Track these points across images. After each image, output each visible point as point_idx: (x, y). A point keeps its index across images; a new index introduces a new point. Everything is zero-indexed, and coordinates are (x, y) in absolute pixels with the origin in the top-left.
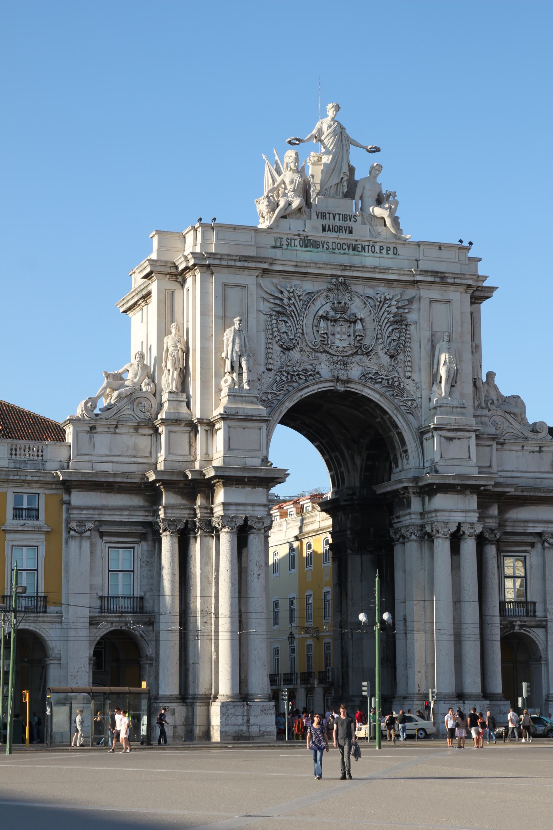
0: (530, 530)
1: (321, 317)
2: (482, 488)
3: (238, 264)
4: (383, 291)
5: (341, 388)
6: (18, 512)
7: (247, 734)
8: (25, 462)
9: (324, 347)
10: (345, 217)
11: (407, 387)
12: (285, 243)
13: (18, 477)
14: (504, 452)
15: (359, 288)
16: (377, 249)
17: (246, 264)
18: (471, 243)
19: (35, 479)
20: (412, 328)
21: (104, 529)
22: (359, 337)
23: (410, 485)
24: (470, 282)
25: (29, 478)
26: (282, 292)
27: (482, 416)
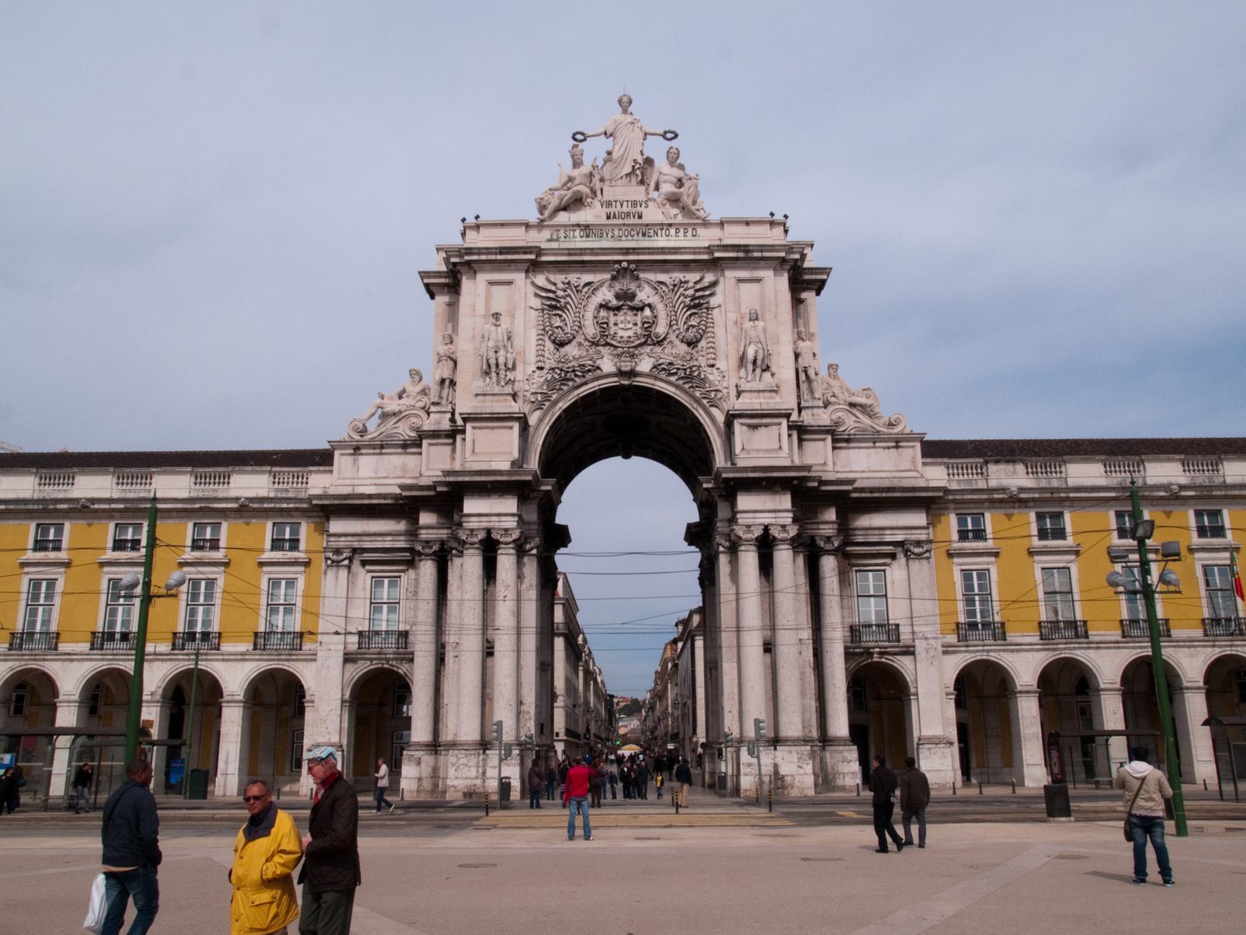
0: (888, 539)
1: (601, 306)
2: (795, 482)
3: (499, 257)
4: (678, 276)
6: (277, 544)
7: (481, 790)
8: (287, 490)
9: (603, 340)
10: (634, 204)
11: (711, 377)
12: (562, 234)
13: (272, 505)
14: (851, 451)
15: (651, 276)
16: (672, 231)
17: (509, 257)
18: (786, 217)
19: (291, 506)
20: (716, 312)
21: (367, 556)
22: (649, 325)
23: (710, 486)
24: (783, 254)
25: (285, 506)
26: (555, 284)
27: (813, 407)
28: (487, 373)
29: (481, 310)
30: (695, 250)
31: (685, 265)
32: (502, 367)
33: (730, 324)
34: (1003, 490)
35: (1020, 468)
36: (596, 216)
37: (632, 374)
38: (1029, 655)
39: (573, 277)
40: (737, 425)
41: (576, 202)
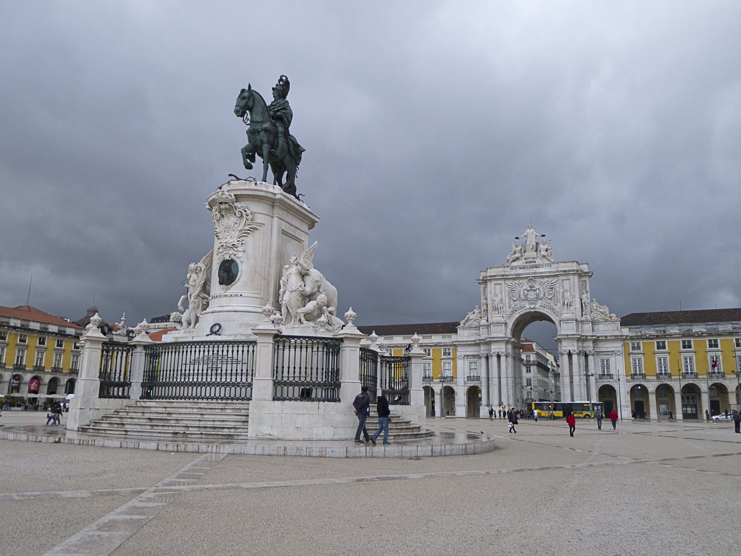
5: (533, 311)
10: (533, 258)
22: (538, 295)
28: (496, 310)
29: (493, 292)
30: (550, 272)
31: (548, 276)
32: (499, 309)
33: (561, 293)
34: (645, 334)
35: (652, 329)
36: (523, 263)
37: (534, 308)
38: (653, 383)
39: (517, 282)
40: (562, 323)
41: (518, 258)
